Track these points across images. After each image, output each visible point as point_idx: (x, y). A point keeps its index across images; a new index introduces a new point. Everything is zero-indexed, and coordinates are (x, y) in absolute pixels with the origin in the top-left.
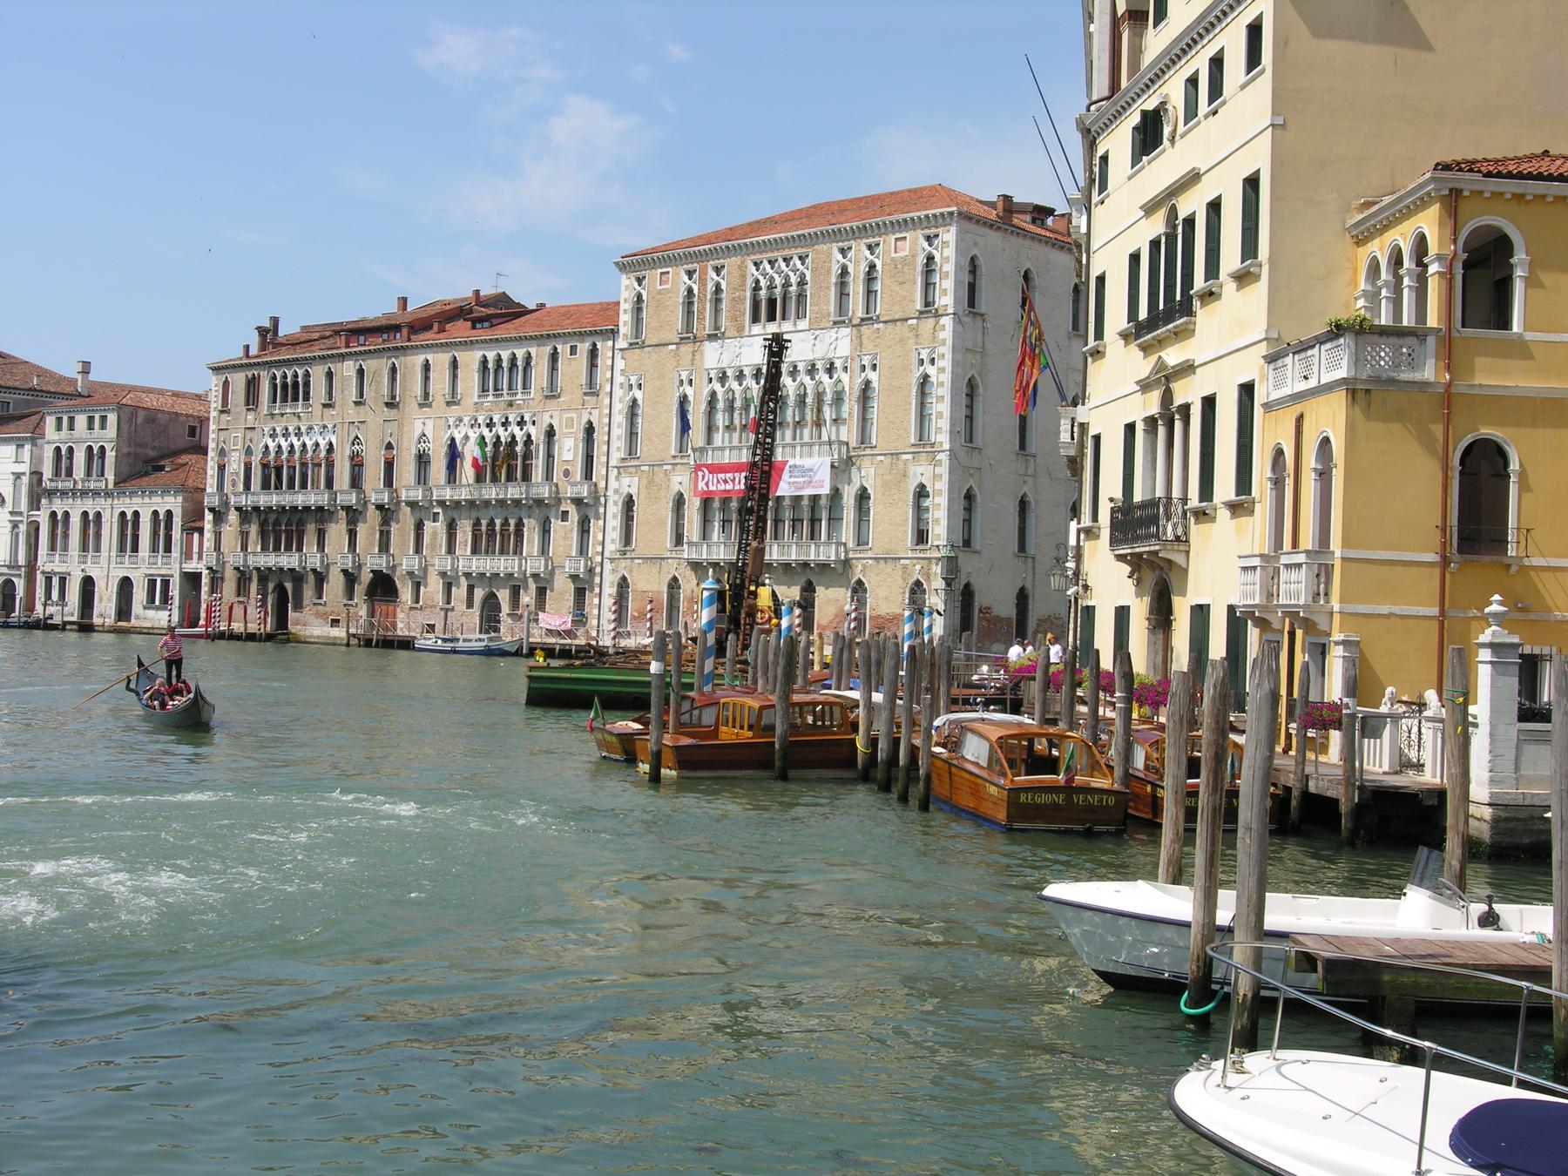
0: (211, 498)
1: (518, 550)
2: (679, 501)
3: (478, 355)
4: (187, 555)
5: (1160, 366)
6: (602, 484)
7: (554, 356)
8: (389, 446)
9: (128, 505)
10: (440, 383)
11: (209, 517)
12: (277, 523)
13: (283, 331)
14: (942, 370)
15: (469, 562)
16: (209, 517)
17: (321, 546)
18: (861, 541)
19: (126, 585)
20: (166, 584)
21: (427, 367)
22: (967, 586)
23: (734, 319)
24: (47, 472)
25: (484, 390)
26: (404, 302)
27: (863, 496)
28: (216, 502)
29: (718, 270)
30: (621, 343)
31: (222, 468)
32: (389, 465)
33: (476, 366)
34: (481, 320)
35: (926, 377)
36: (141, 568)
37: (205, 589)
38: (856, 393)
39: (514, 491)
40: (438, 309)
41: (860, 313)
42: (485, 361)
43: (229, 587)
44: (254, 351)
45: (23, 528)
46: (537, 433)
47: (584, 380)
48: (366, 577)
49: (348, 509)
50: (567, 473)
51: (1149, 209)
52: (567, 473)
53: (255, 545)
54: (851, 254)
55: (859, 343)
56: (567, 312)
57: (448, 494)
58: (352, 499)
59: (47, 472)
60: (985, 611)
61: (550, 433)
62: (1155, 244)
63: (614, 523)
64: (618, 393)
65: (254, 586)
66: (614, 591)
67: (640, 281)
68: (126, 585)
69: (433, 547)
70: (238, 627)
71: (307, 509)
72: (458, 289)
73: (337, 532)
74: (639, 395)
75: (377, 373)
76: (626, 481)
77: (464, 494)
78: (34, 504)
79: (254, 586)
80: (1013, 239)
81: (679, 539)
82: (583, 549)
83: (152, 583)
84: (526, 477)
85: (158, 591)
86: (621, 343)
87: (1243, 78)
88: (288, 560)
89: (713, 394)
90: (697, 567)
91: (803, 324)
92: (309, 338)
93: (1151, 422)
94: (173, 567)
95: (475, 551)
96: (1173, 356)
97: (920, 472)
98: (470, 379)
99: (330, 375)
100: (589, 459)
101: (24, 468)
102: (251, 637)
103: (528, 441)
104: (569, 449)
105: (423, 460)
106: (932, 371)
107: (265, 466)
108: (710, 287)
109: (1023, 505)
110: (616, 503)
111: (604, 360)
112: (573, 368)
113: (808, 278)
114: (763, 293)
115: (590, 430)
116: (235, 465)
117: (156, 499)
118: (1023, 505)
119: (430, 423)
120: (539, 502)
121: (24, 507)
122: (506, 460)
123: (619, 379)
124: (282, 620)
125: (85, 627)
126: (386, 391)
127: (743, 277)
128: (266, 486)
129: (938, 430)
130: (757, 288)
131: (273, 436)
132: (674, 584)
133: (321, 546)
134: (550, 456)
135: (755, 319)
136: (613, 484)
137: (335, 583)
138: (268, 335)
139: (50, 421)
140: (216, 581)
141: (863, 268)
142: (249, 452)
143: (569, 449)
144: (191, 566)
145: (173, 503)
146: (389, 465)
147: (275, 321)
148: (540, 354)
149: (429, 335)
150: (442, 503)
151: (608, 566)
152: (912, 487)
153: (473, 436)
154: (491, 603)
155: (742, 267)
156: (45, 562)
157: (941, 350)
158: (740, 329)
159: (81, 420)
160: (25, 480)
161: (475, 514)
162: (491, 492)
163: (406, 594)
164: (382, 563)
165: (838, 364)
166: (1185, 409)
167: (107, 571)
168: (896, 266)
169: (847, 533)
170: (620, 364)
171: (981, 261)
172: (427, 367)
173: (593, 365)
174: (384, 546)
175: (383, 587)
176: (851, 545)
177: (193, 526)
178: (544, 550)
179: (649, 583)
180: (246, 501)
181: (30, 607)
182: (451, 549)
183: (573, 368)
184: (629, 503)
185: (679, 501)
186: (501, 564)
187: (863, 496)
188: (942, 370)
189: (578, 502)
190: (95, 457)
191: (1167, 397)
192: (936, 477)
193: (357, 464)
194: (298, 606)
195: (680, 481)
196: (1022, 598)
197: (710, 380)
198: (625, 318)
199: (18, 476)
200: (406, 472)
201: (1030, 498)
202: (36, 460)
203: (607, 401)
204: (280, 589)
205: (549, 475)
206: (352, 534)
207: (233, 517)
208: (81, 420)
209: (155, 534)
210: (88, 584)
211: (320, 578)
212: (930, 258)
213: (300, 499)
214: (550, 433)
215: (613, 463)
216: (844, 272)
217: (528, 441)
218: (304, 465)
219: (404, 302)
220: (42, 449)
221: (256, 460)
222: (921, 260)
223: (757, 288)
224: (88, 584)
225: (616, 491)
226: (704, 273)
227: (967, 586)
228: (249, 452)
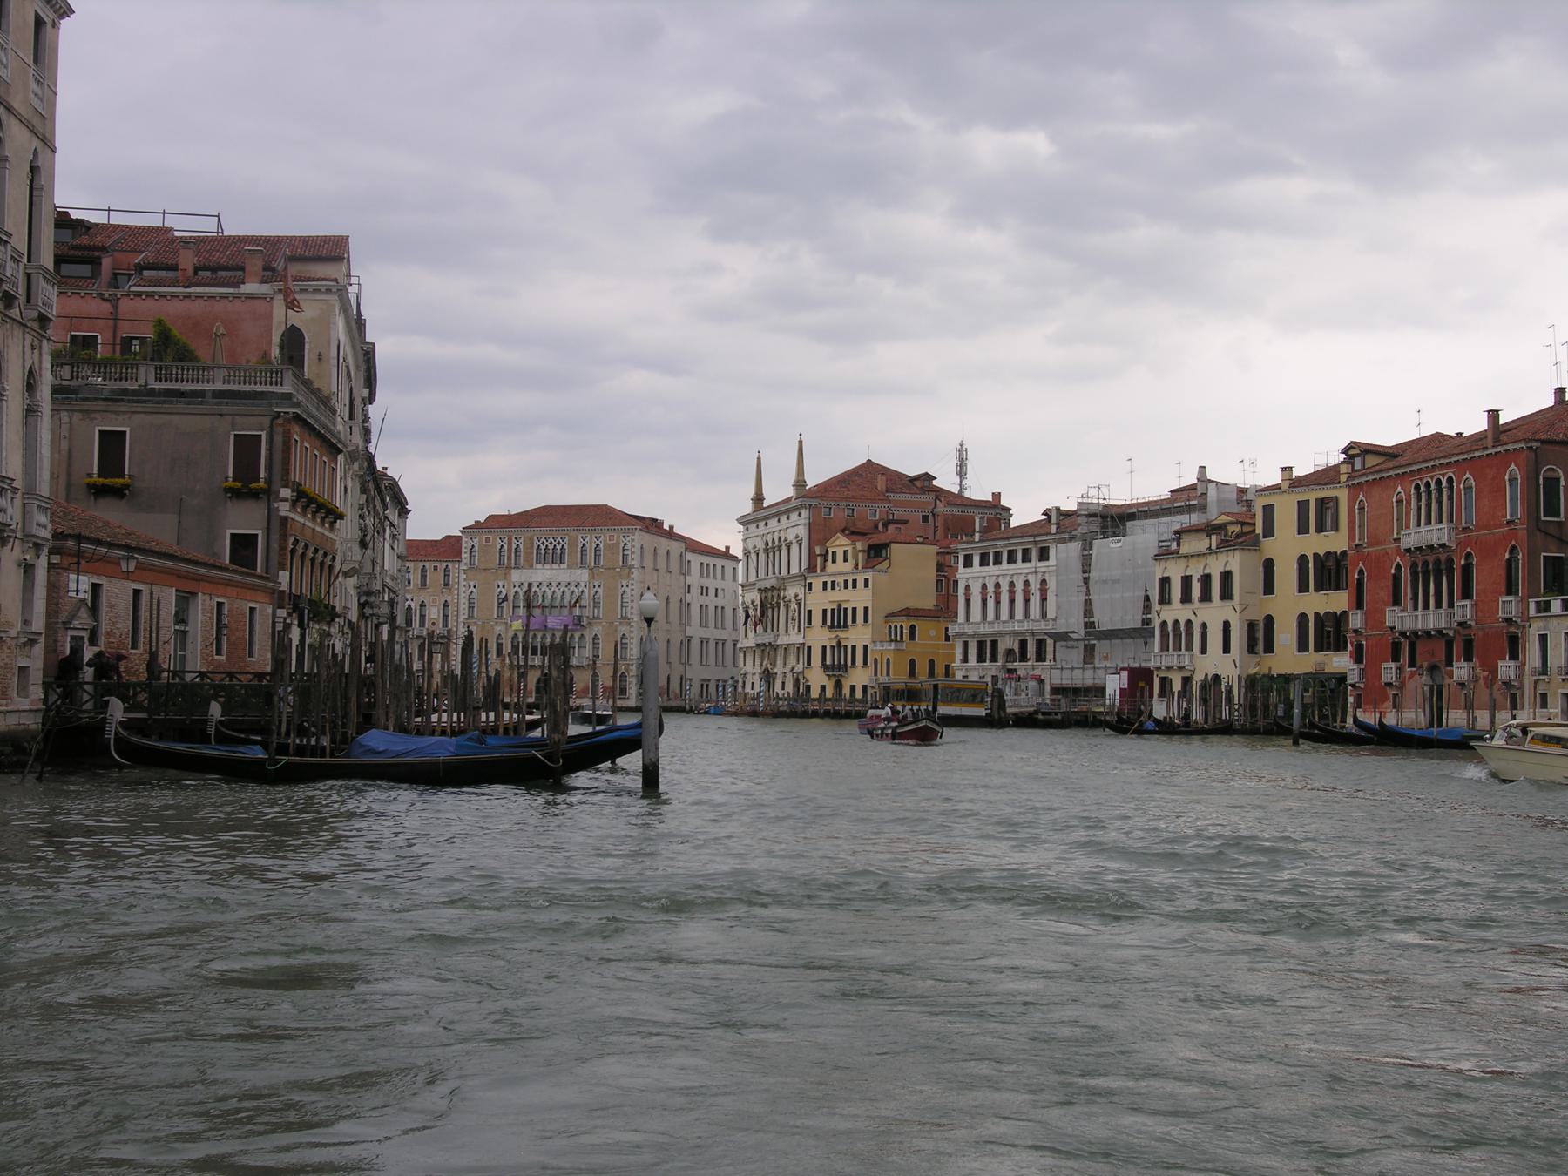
55: (592, 577)
61: (422, 605)
97: (623, 630)
100: (446, 616)
104: (434, 613)
115: (446, 605)
134: (423, 616)
143: (434, 613)
155: (531, 539)
187: (595, 638)
205: (422, 624)
214: (422, 605)
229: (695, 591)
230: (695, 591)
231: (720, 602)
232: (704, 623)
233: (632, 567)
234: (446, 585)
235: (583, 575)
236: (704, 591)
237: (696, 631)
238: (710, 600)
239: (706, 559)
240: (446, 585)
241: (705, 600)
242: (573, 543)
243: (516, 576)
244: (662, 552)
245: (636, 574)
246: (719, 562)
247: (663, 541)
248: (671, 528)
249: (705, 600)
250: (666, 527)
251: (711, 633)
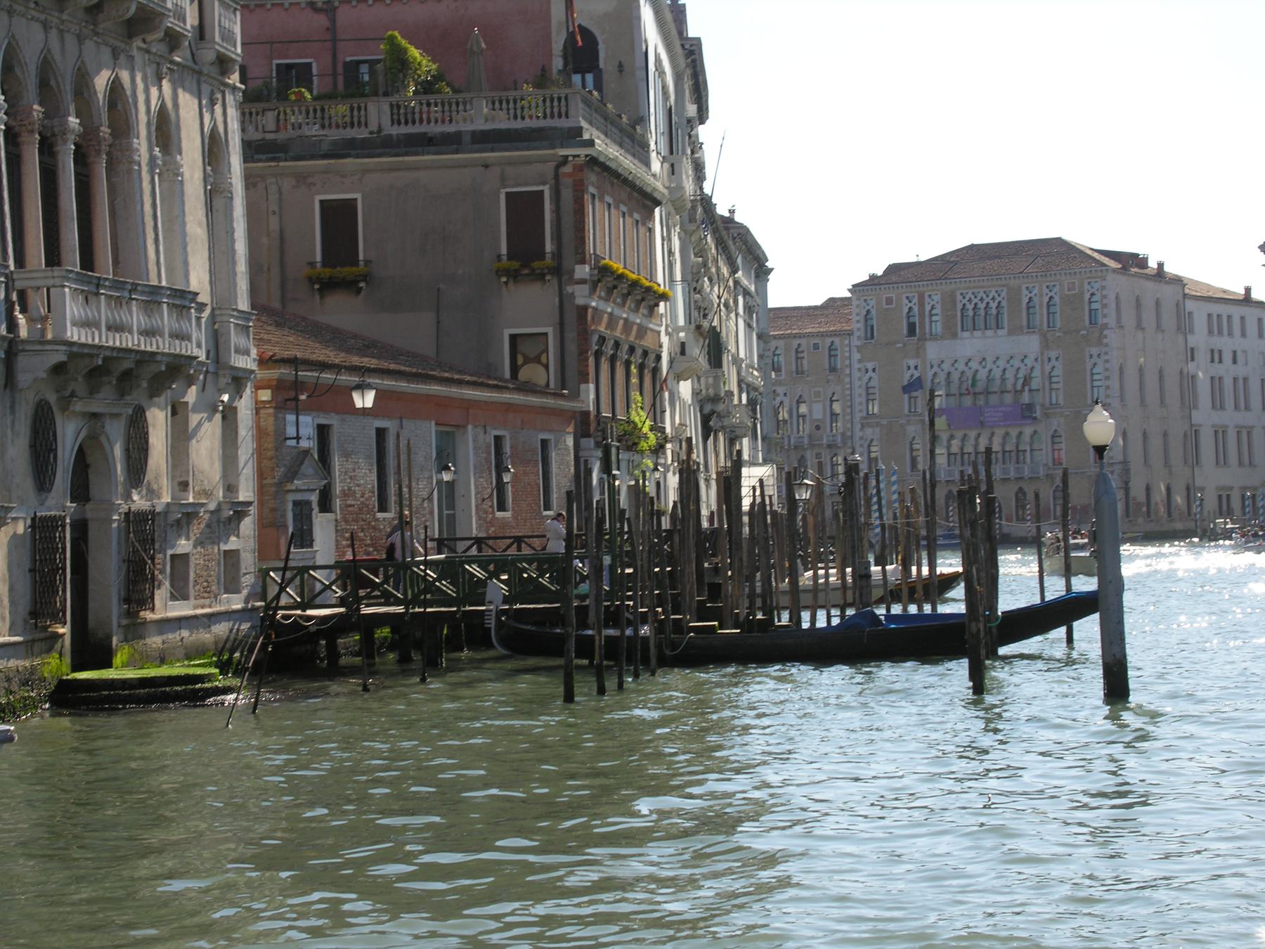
6: (849, 434)
52: (818, 428)
60: (1134, 498)
64: (856, 374)
91: (1000, 332)
108: (928, 308)
110: (861, 446)
113: (1004, 303)
123: (857, 366)
127: (954, 302)
136: (858, 434)
141: (1046, 299)
197: (932, 367)
203: (847, 380)
225: (861, 438)
229: (1202, 356)
230: (1202, 356)
231: (1240, 370)
232: (1218, 404)
233: (1105, 326)
235: (1031, 344)
236: (1215, 356)
237: (1205, 416)
238: (1226, 370)
239: (1216, 309)
241: (1218, 369)
244: (1148, 304)
245: (1112, 338)
246: (1237, 312)
247: (1150, 285)
248: (1161, 265)
249: (1218, 369)
250: (1152, 264)
251: (1229, 417)
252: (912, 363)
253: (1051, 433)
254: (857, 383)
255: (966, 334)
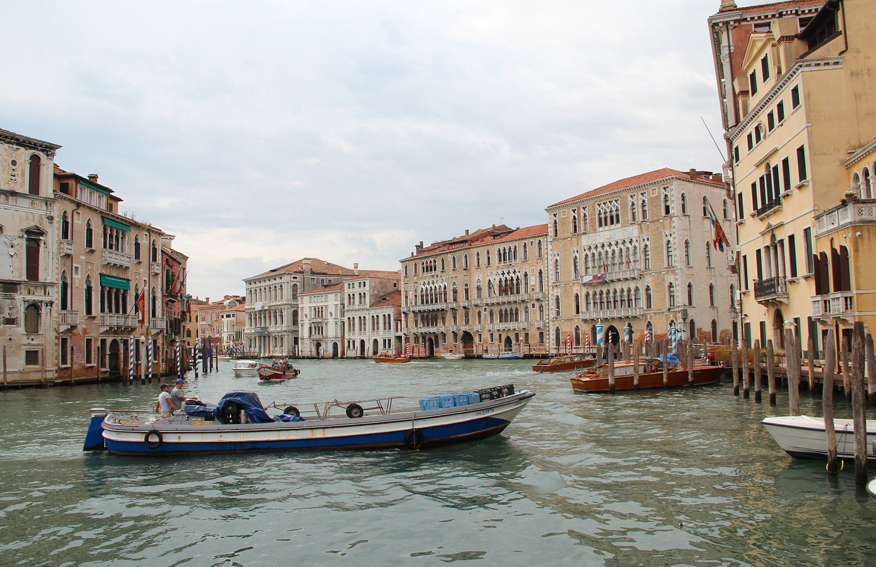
0: (404, 308)
1: (517, 320)
2: (577, 296)
3: (496, 247)
4: (397, 330)
5: (769, 226)
7: (525, 245)
8: (466, 285)
9: (374, 312)
10: (484, 260)
11: (403, 315)
12: (427, 316)
13: (426, 245)
14: (675, 238)
15: (498, 325)
16: (403, 315)
17: (444, 323)
18: (649, 306)
19: (376, 341)
20: (389, 340)
21: (478, 254)
22: (692, 320)
23: (592, 226)
24: (346, 303)
25: (500, 260)
26: (467, 231)
27: (648, 289)
28: (406, 310)
29: (584, 208)
30: (550, 239)
31: (406, 297)
32: (467, 290)
33: (497, 252)
34: (497, 235)
35: (669, 241)
36: (381, 335)
37: (403, 342)
38: (642, 249)
39: (512, 298)
40: (480, 233)
41: (641, 219)
42: (499, 251)
43: (412, 340)
44: (415, 254)
45: (339, 323)
46: (521, 276)
47: (537, 254)
48: (460, 334)
49: (453, 309)
50: (533, 290)
51: (758, 166)
52: (533, 290)
53: (420, 324)
54: (635, 197)
56: (528, 229)
57: (489, 301)
58: (454, 305)
59: (346, 303)
60: (700, 330)
61: (526, 275)
62: (762, 179)
63: (553, 306)
64: (550, 258)
65: (421, 340)
66: (554, 332)
67: (555, 215)
68: (376, 341)
69: (485, 321)
70: (416, 355)
71: (438, 310)
72: (487, 226)
73: (449, 316)
74: (558, 258)
75: (460, 259)
76: (555, 290)
77: (495, 301)
78: (343, 315)
79: (421, 340)
80: (697, 185)
81: (578, 312)
82: (541, 318)
83: (385, 341)
84: (518, 292)
85: (387, 343)
86: (550, 239)
87: (792, 111)
88: (432, 330)
89: (587, 255)
90: (585, 321)
91: (619, 225)
92: (436, 246)
93: (767, 248)
94: (392, 335)
95: (501, 321)
96: (774, 221)
97: (670, 278)
98: (495, 258)
99: (443, 260)
101: (338, 303)
102: (422, 358)
103: (518, 279)
104: (533, 280)
105: (479, 289)
106: (671, 239)
107: (422, 296)
108: (582, 215)
109: (711, 287)
111: (543, 247)
112: (533, 251)
114: (602, 216)
115: (541, 273)
116: (411, 296)
117: (384, 310)
118: (711, 287)
119: (481, 275)
120: (523, 301)
121: (339, 316)
122: (508, 287)
123: (550, 253)
124: (432, 351)
125: (363, 357)
126: (464, 265)
128: (422, 303)
129: (675, 261)
130: (600, 214)
131: (424, 284)
132: (577, 328)
133: (444, 323)
134: (526, 284)
135: (600, 225)
136: (551, 292)
137: (450, 337)
138: (420, 248)
139: (346, 286)
140: (407, 340)
142: (416, 291)
143: (533, 280)
144: (399, 334)
145: (390, 311)
146: (467, 290)
147: (422, 243)
148: (520, 245)
149: (478, 243)
150: (487, 304)
151: (551, 323)
152: (667, 284)
153: (497, 279)
154: (508, 340)
155: (593, 207)
156: (347, 336)
157: (674, 230)
158: (595, 230)
159: (356, 284)
160: (339, 306)
161: (499, 308)
162: (505, 299)
163: (476, 339)
164: (466, 328)
165: (634, 239)
166: (782, 241)
167: (369, 337)
168: (652, 200)
169: (643, 303)
170: (550, 247)
171: (686, 195)
172: (478, 254)
173: (540, 249)
174: (467, 322)
175: (467, 338)
176: (645, 308)
177: (398, 320)
178: (527, 319)
179: (568, 329)
180: (416, 309)
181: (343, 353)
182: (492, 322)
183: (533, 251)
184: (557, 299)
185: (577, 296)
186: (511, 325)
187: (648, 289)
188: (675, 238)
189: (538, 300)
190: (362, 296)
191: (773, 237)
192: (676, 279)
193: (455, 292)
194: (437, 346)
195: (576, 289)
196: (714, 323)
198: (551, 230)
199: (336, 305)
200: (473, 293)
201: (714, 284)
202: (342, 299)
204: (430, 340)
205: (526, 291)
206: (455, 318)
207: (411, 315)
208: (356, 284)
209: (385, 323)
210: (363, 342)
211: (444, 335)
212: (666, 196)
213: (435, 307)
214: (526, 275)
215: (550, 284)
216: (633, 204)
217: (518, 279)
218: (436, 295)
219: (467, 231)
220: (343, 295)
221: (419, 294)
222: (663, 197)
223: (600, 214)
224: (363, 342)
226: (579, 208)
227: (692, 320)
228: (416, 291)
234: (540, 255)
235: (633, 232)
240: (540, 255)
242: (624, 205)
243: (585, 241)
252: (575, 249)
253: (645, 287)
254: (550, 263)
255: (601, 229)
